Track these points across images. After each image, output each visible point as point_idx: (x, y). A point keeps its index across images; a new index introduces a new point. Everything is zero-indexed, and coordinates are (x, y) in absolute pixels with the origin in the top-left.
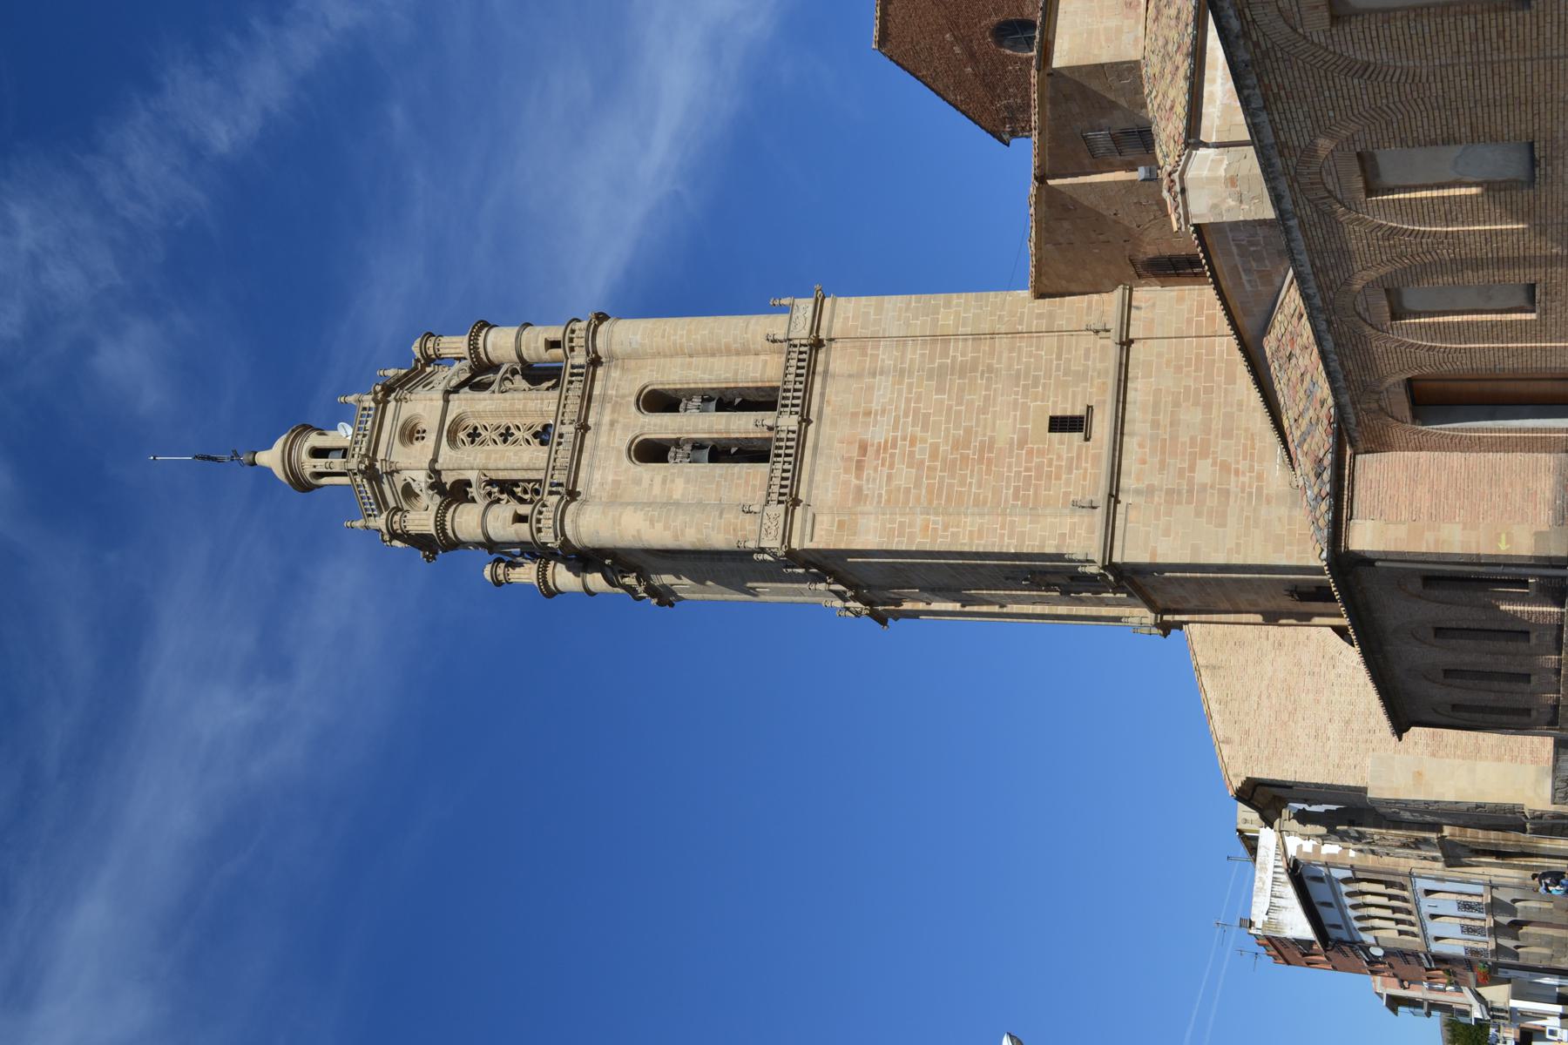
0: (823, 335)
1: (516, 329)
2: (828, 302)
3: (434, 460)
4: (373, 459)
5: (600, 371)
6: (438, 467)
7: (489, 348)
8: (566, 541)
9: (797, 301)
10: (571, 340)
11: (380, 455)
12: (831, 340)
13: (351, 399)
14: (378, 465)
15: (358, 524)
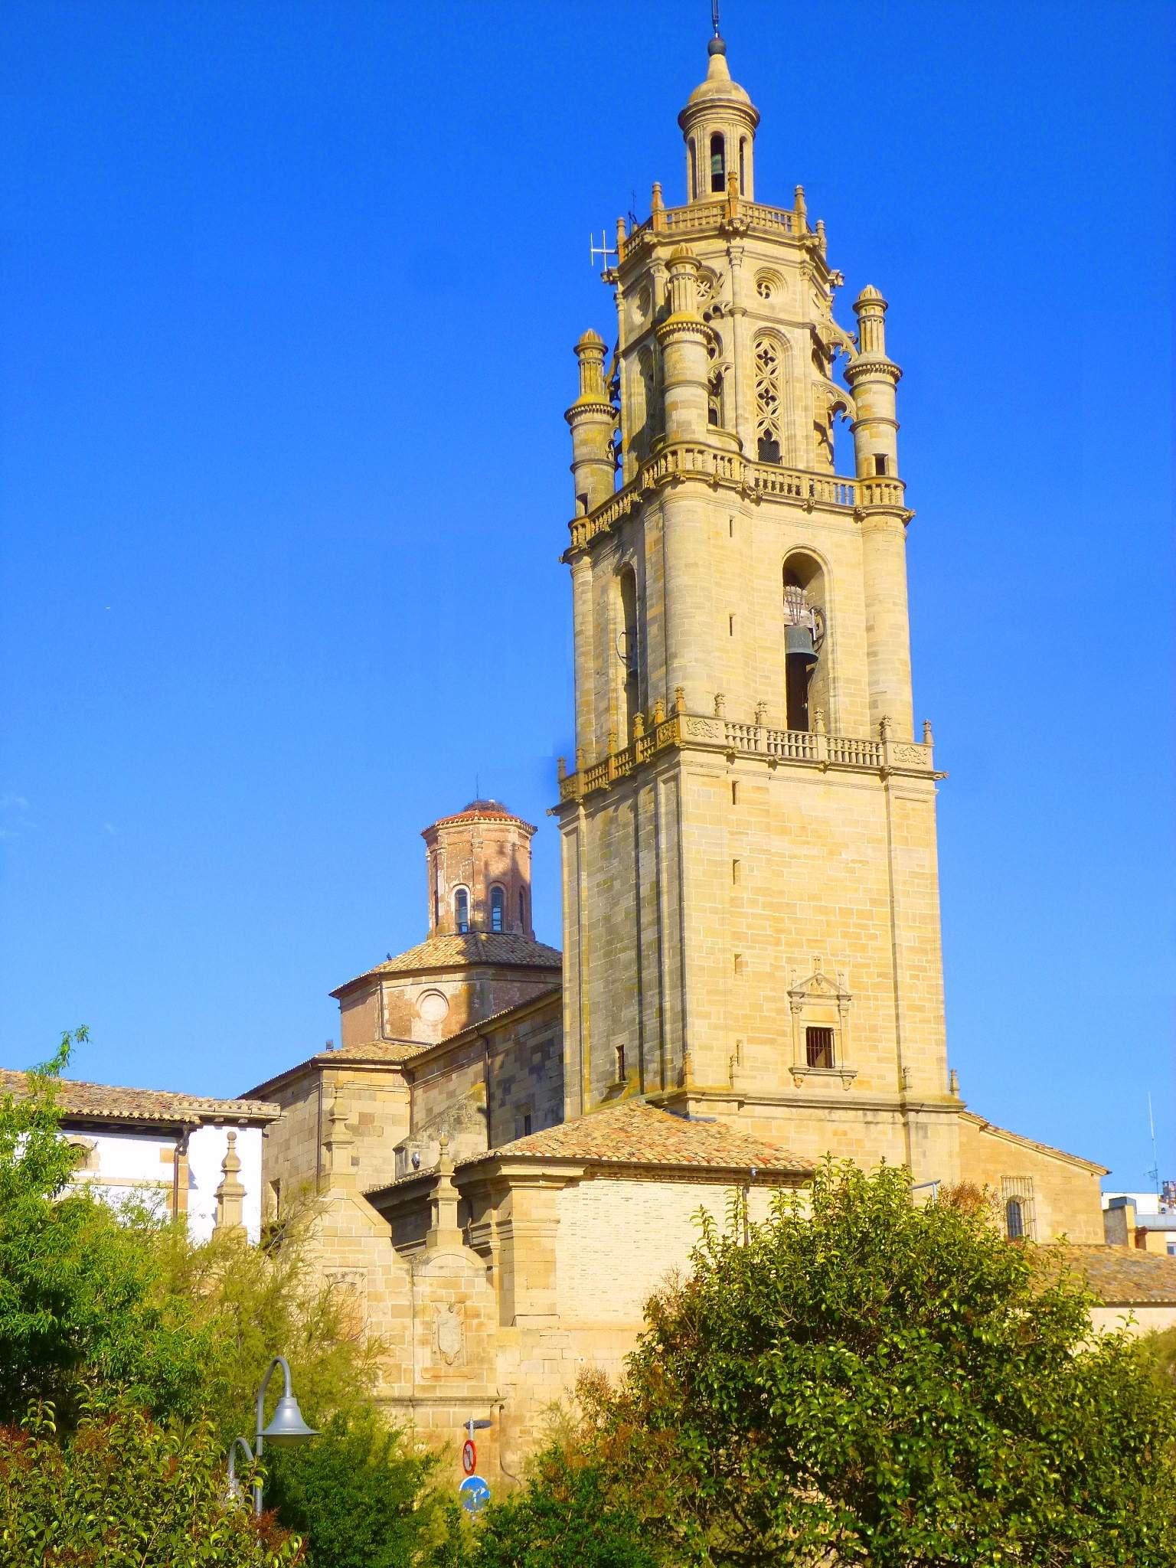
0: (892, 780)
1: (893, 418)
2: (929, 785)
3: (744, 313)
4: (743, 235)
5: (850, 520)
6: (738, 316)
7: (875, 387)
8: (676, 481)
9: (930, 751)
10: (887, 486)
11: (747, 243)
12: (887, 789)
13: (803, 207)
14: (737, 242)
15: (661, 205)
